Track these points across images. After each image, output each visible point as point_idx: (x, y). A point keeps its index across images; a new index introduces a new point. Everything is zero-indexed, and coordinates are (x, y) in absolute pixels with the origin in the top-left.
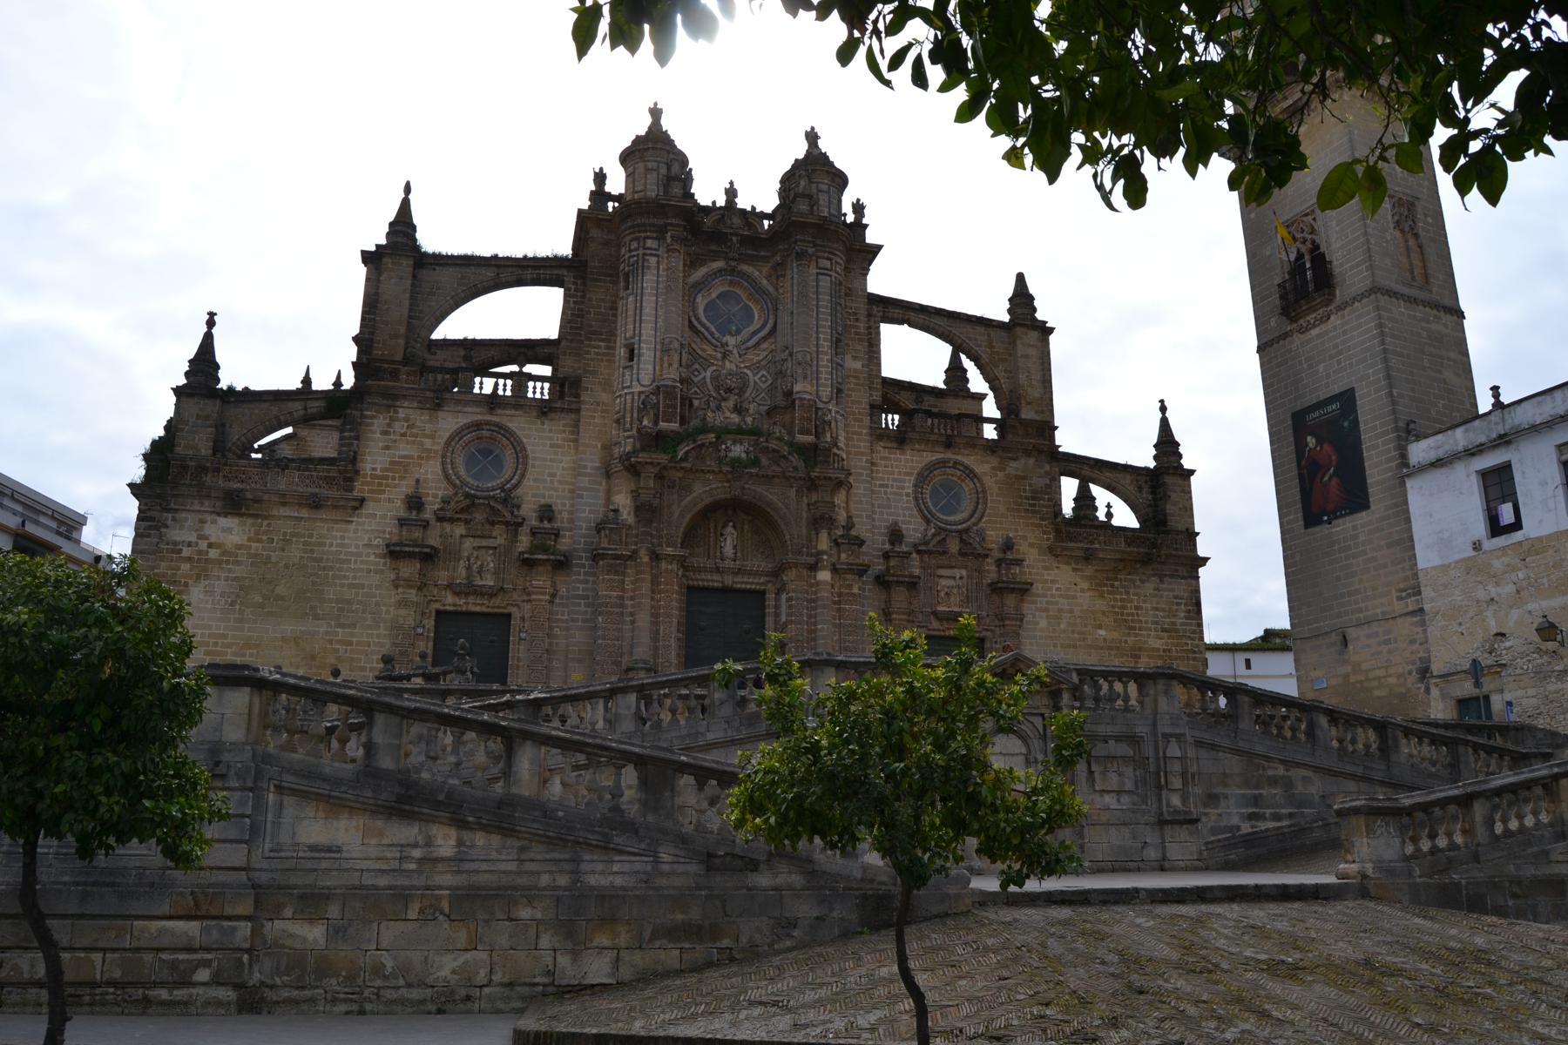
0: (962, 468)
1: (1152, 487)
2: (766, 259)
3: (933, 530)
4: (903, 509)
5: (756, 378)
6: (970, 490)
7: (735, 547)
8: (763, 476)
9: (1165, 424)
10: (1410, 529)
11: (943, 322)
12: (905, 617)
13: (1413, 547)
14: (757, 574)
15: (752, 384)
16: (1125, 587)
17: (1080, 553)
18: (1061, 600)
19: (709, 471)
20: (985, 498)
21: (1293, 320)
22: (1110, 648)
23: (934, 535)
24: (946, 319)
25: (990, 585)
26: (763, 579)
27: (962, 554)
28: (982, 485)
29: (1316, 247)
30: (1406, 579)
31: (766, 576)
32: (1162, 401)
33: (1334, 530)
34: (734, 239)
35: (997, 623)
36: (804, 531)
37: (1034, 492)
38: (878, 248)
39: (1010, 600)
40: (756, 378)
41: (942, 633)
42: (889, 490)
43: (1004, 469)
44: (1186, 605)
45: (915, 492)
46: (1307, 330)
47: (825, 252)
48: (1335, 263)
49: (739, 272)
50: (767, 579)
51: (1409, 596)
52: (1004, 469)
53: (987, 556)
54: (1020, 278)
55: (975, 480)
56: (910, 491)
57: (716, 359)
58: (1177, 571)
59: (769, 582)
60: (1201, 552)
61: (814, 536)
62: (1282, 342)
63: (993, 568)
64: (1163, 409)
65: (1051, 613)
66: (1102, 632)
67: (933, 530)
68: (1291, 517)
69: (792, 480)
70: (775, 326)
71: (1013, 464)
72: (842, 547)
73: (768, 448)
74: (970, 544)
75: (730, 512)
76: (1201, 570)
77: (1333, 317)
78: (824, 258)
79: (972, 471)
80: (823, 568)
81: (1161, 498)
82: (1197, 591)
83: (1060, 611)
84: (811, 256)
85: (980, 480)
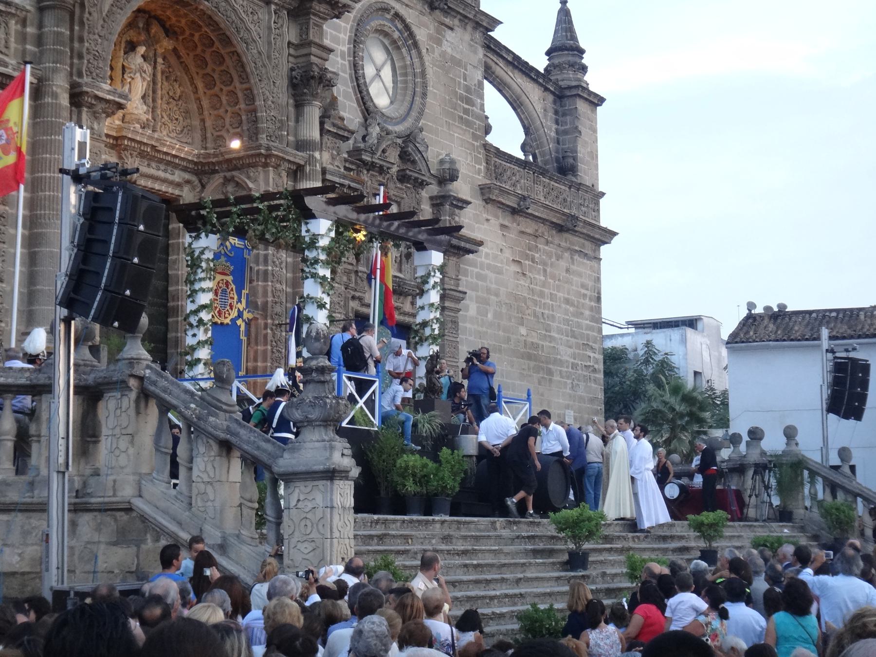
0: (400, 26)
1: (556, 112)
6: (405, 67)
16: (544, 264)
17: (512, 202)
20: (425, 85)
23: (380, 138)
27: (403, 178)
28: (422, 64)
31: (185, 169)
37: (468, 89)
44: (591, 300)
50: (187, 176)
52: (439, 42)
53: (421, 184)
55: (413, 52)
56: (345, 49)
60: (606, 220)
61: (292, 109)
65: (480, 294)
66: (523, 331)
67: (378, 129)
71: (449, 35)
74: (414, 162)
76: (604, 249)
79: (412, 35)
81: (565, 132)
82: (598, 280)
83: (488, 290)
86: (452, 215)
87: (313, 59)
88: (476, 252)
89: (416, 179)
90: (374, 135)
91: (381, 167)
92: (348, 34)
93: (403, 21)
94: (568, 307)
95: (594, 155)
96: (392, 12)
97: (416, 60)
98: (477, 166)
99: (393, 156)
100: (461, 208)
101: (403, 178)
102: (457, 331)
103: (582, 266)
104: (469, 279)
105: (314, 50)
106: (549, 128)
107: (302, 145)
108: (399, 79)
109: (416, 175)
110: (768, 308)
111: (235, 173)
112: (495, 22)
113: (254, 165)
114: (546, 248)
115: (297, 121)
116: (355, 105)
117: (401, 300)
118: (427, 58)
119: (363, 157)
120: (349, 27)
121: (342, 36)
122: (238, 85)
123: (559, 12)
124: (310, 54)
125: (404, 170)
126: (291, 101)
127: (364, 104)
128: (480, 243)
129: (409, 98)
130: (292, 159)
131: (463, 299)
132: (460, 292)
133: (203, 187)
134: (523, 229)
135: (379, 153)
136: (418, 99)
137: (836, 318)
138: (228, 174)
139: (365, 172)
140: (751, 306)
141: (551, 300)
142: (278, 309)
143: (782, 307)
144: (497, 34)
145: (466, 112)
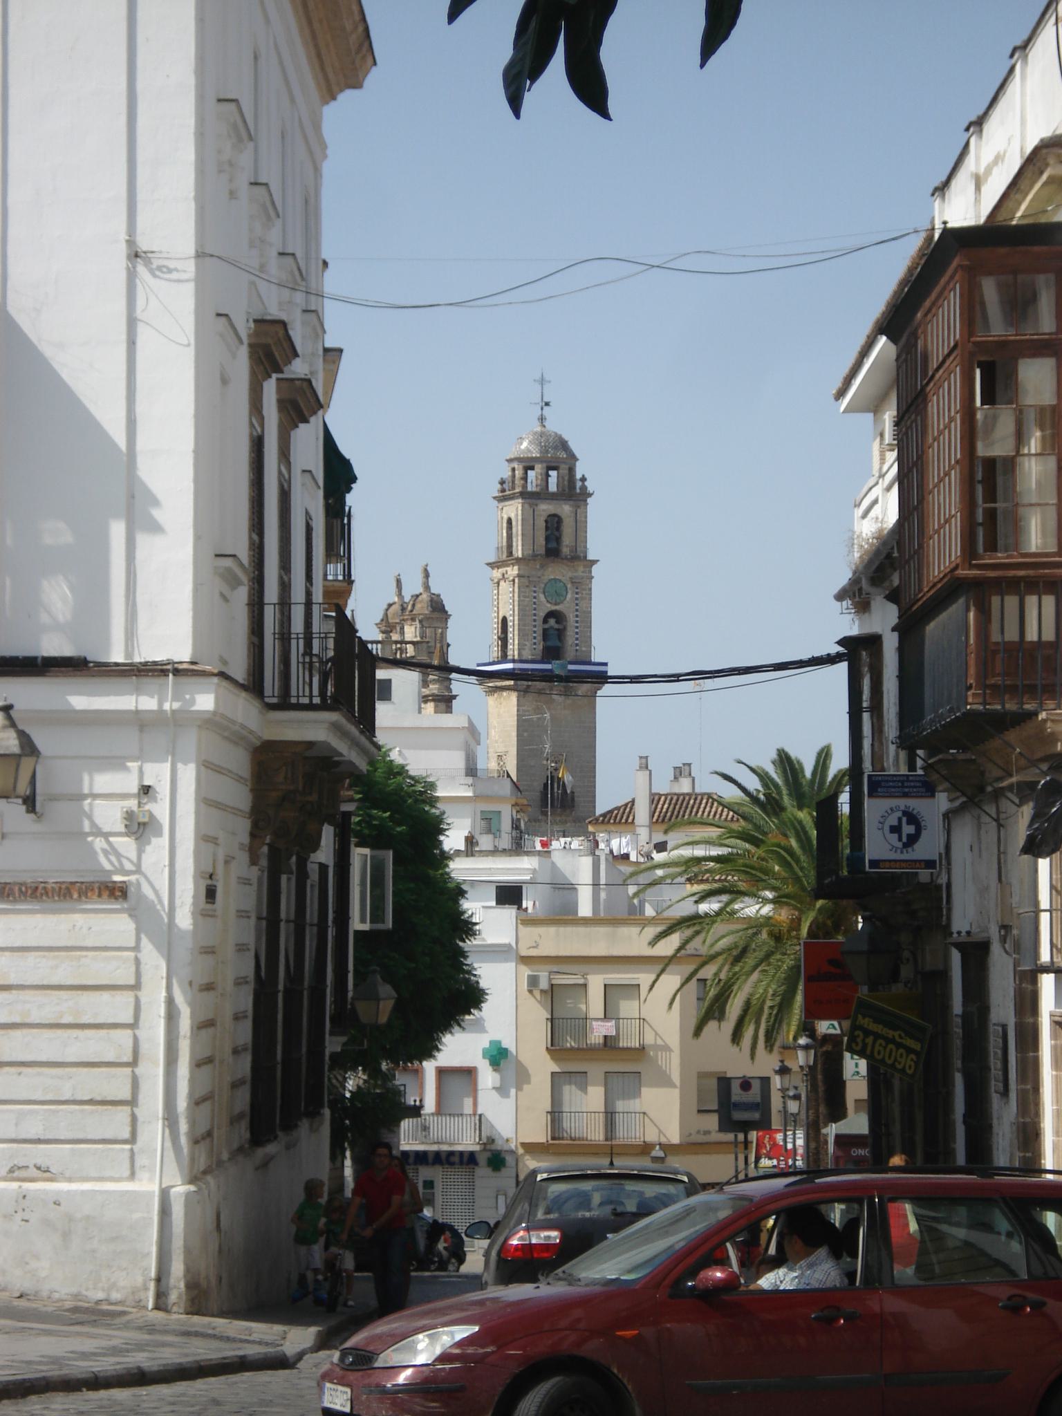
62: (534, 824)
77: (569, 824)
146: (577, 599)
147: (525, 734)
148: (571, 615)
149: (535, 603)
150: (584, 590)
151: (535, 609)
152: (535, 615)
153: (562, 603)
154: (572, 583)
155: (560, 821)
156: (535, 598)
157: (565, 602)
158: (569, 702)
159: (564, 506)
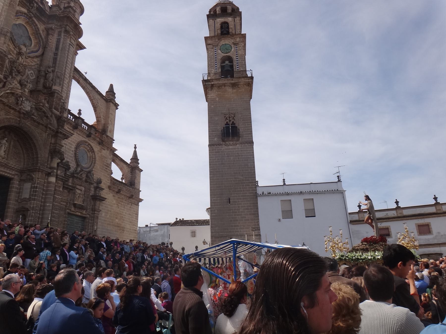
0: (90, 147)
2: (44, 23)
3: (80, 169)
4: (70, 156)
5: (29, 73)
7: (4, 151)
8: (37, 122)
9: (135, 153)
10: (258, 211)
11: (90, 88)
12: (65, 204)
13: (258, 216)
14: (12, 169)
15: (26, 74)
18: (109, 207)
19: (13, 109)
20: (95, 161)
21: (223, 141)
22: (118, 227)
23: (80, 171)
24: (91, 87)
25: (91, 196)
26: (13, 173)
27: (86, 181)
28: (95, 156)
29: (233, 123)
30: (255, 225)
31: (16, 171)
32: (135, 145)
33: (231, 206)
34: (35, 5)
35: (91, 212)
36: (47, 156)
37: (107, 164)
38: (85, 48)
39: (98, 203)
40: (29, 73)
41: (74, 213)
42: (67, 147)
43: (101, 152)
45: (76, 151)
46: (228, 146)
47: (74, 37)
48: (240, 131)
49: (33, 20)
50: (17, 173)
51: (256, 230)
52: (101, 152)
53: (92, 184)
54: (111, 86)
56: (73, 150)
57: (13, 53)
58: (135, 202)
59: (17, 175)
60: (141, 197)
61: (50, 159)
62: (218, 146)
63: (93, 189)
64: (135, 148)
66: (117, 220)
67: (80, 169)
68: (215, 199)
69: (48, 129)
70: (43, 54)
71: (103, 151)
72: (59, 168)
73: (42, 109)
74: (90, 178)
75: (7, 133)
77: (238, 145)
78: (73, 39)
79: (93, 149)
80: (52, 176)
83: (108, 210)
84: (70, 35)
85: (95, 154)
86: (99, 191)
87: (57, 147)
88: (104, 201)
89: (90, 182)
90: (79, 170)
91: (80, 178)
92: (75, 146)
93: (91, 146)
94: (130, 216)
95: (139, 182)
96: (88, 143)
97: (93, 155)
98: (108, 181)
99: (84, 176)
100: (102, 190)
101: (86, 181)
102: (98, 219)
103: (134, 206)
104: (103, 207)
105: (58, 145)
106: (129, 175)
107: (51, 168)
108: (89, 159)
109: (90, 181)
110: (180, 219)
111: (30, 173)
112: (116, 150)
113: (36, 171)
114: (125, 202)
115: (51, 162)
116: (75, 163)
117: (82, 211)
118: (97, 156)
119: (75, 175)
120: (75, 145)
121: (73, 146)
122: (34, 151)
123: (134, 151)
124: (57, 146)
125: (87, 180)
126: (50, 157)
127: (77, 163)
128: (106, 199)
129: (90, 164)
130: (46, 170)
131: (100, 212)
132: (99, 210)
133: (22, 176)
134: (119, 197)
135: (79, 175)
136: (93, 164)
137: (194, 222)
138: (28, 173)
139: (75, 179)
140: (177, 219)
141: (125, 214)
142: (37, 208)
143: (183, 219)
144: (116, 152)
145: (106, 169)
146: (236, 50)
147: (212, 106)
148: (234, 57)
149: (215, 54)
150: (241, 46)
151: (216, 56)
152: (216, 58)
153: (229, 52)
154: (234, 44)
155: (233, 144)
156: (215, 51)
157: (231, 52)
158: (234, 91)
159: (228, 18)
